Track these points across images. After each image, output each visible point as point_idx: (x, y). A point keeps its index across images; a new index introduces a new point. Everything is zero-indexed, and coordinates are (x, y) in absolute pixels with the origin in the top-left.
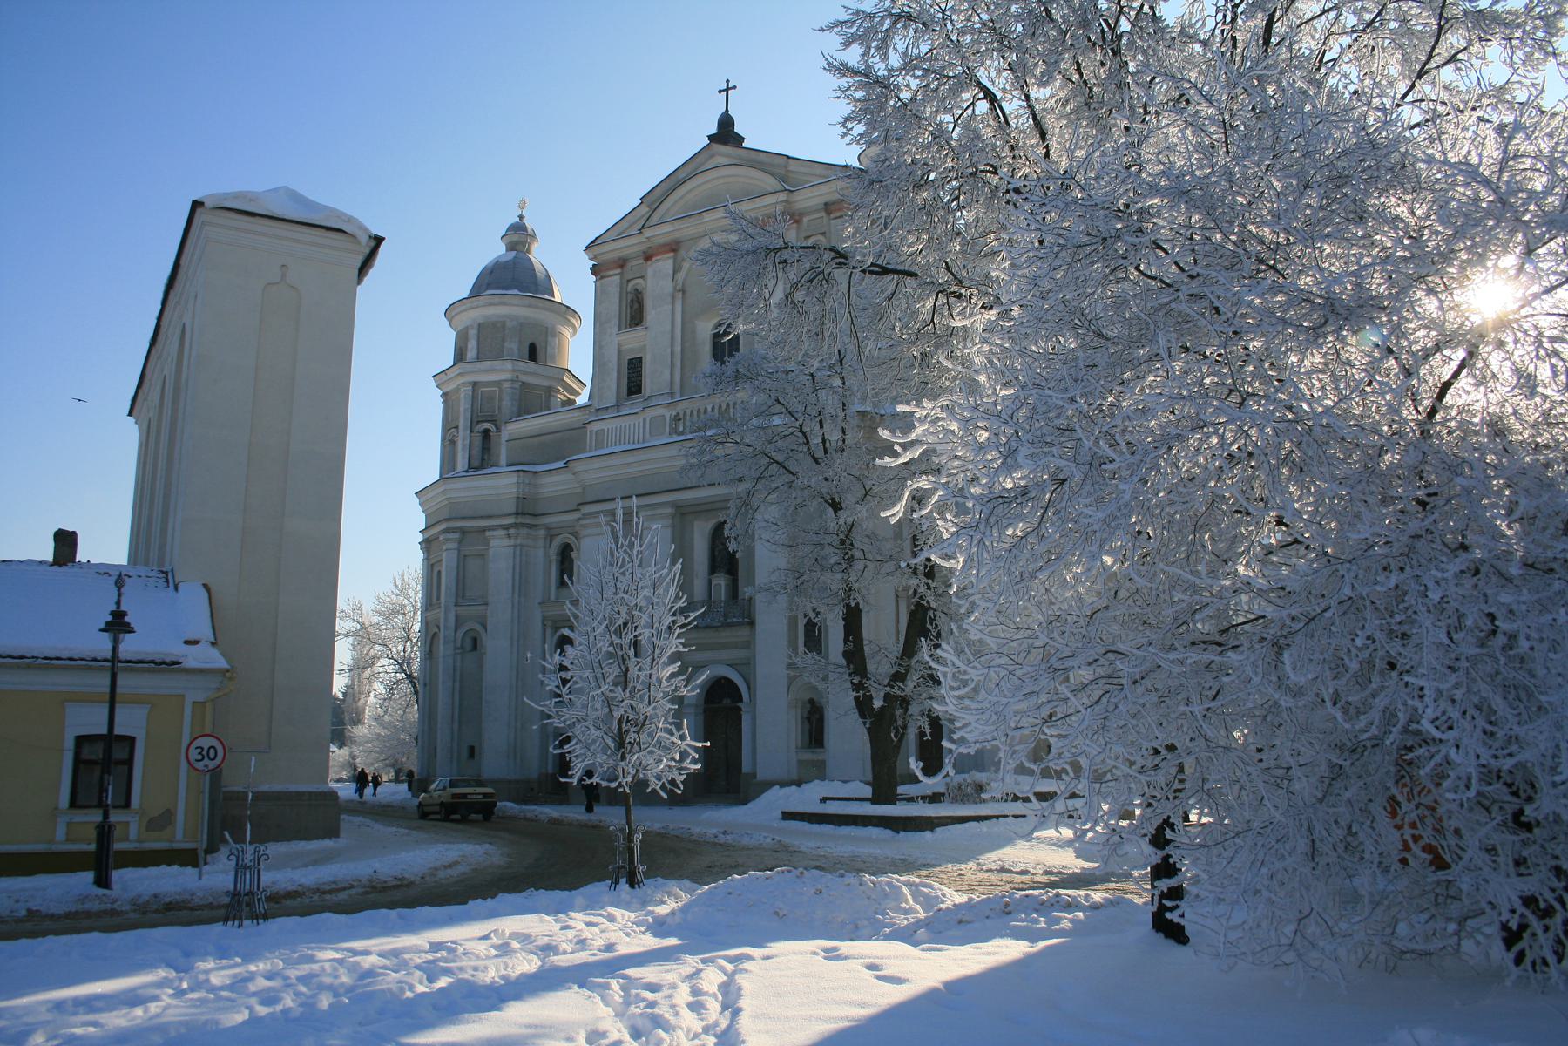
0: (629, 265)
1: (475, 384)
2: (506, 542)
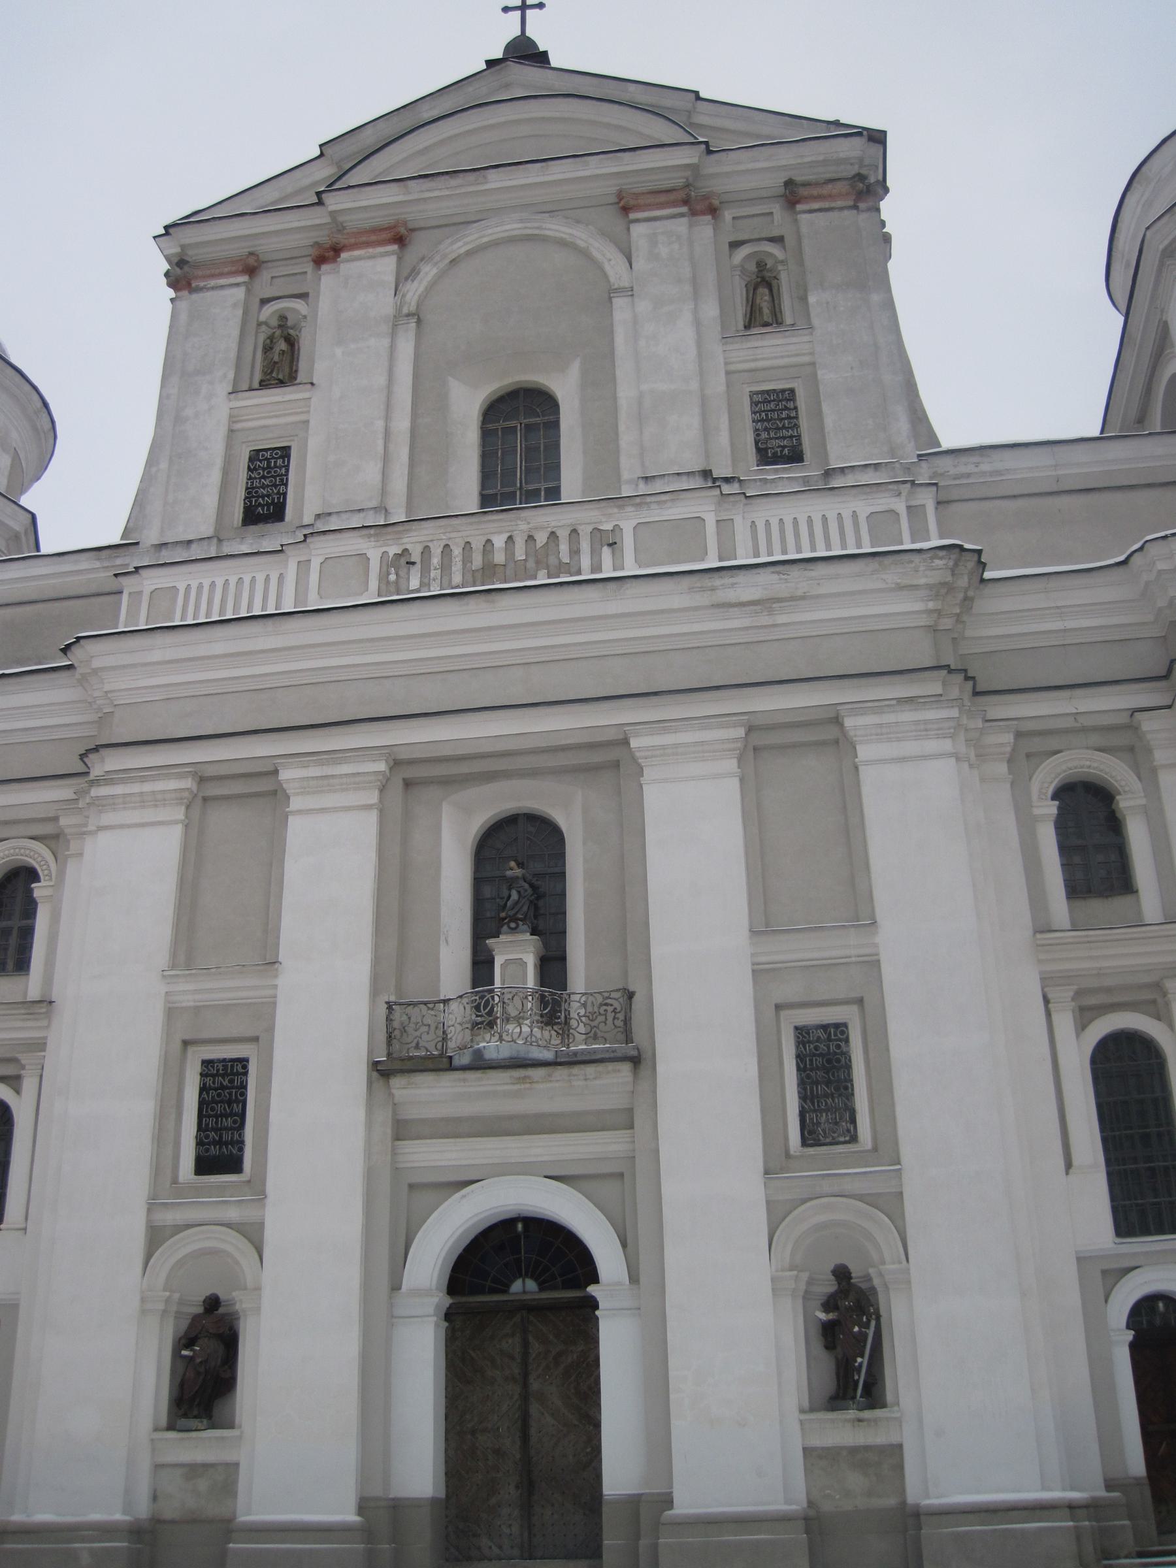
0: (265, 275)
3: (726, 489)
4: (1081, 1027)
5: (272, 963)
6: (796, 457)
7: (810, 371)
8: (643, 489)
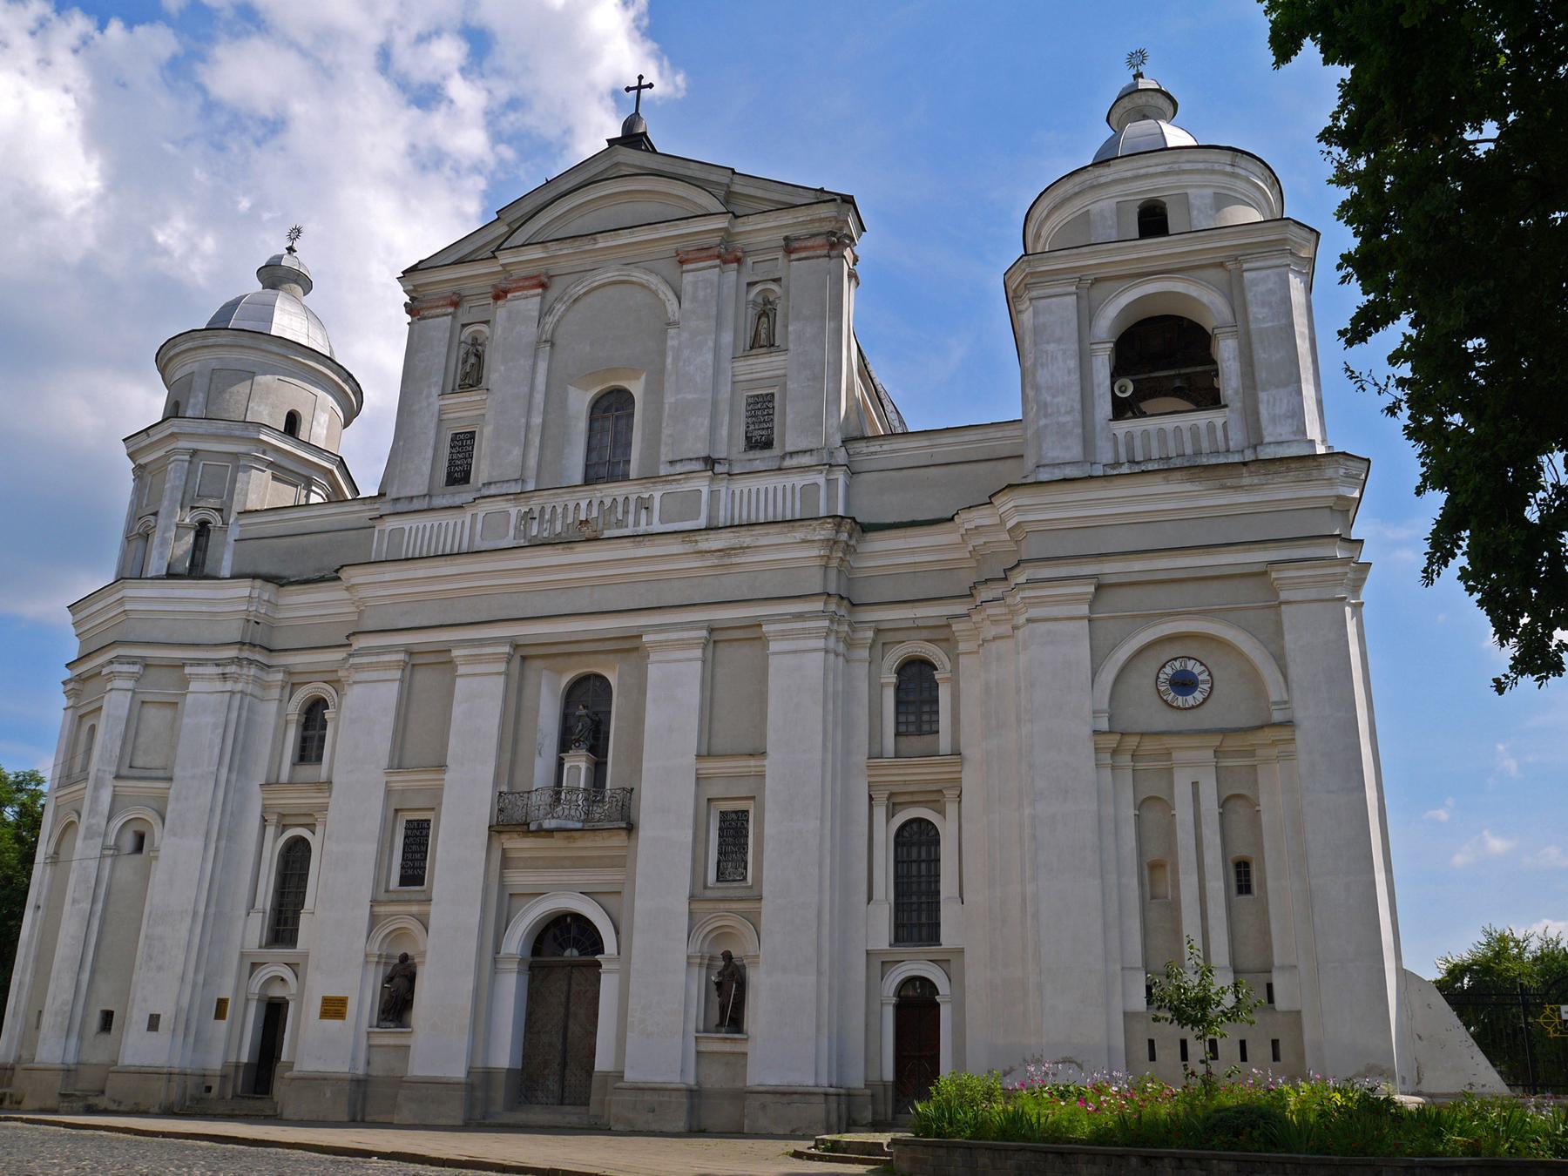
0: (466, 306)
1: (194, 453)
2: (219, 686)
3: (718, 468)
4: (891, 814)
5: (441, 767)
6: (768, 444)
7: (782, 380)
8: (672, 470)
